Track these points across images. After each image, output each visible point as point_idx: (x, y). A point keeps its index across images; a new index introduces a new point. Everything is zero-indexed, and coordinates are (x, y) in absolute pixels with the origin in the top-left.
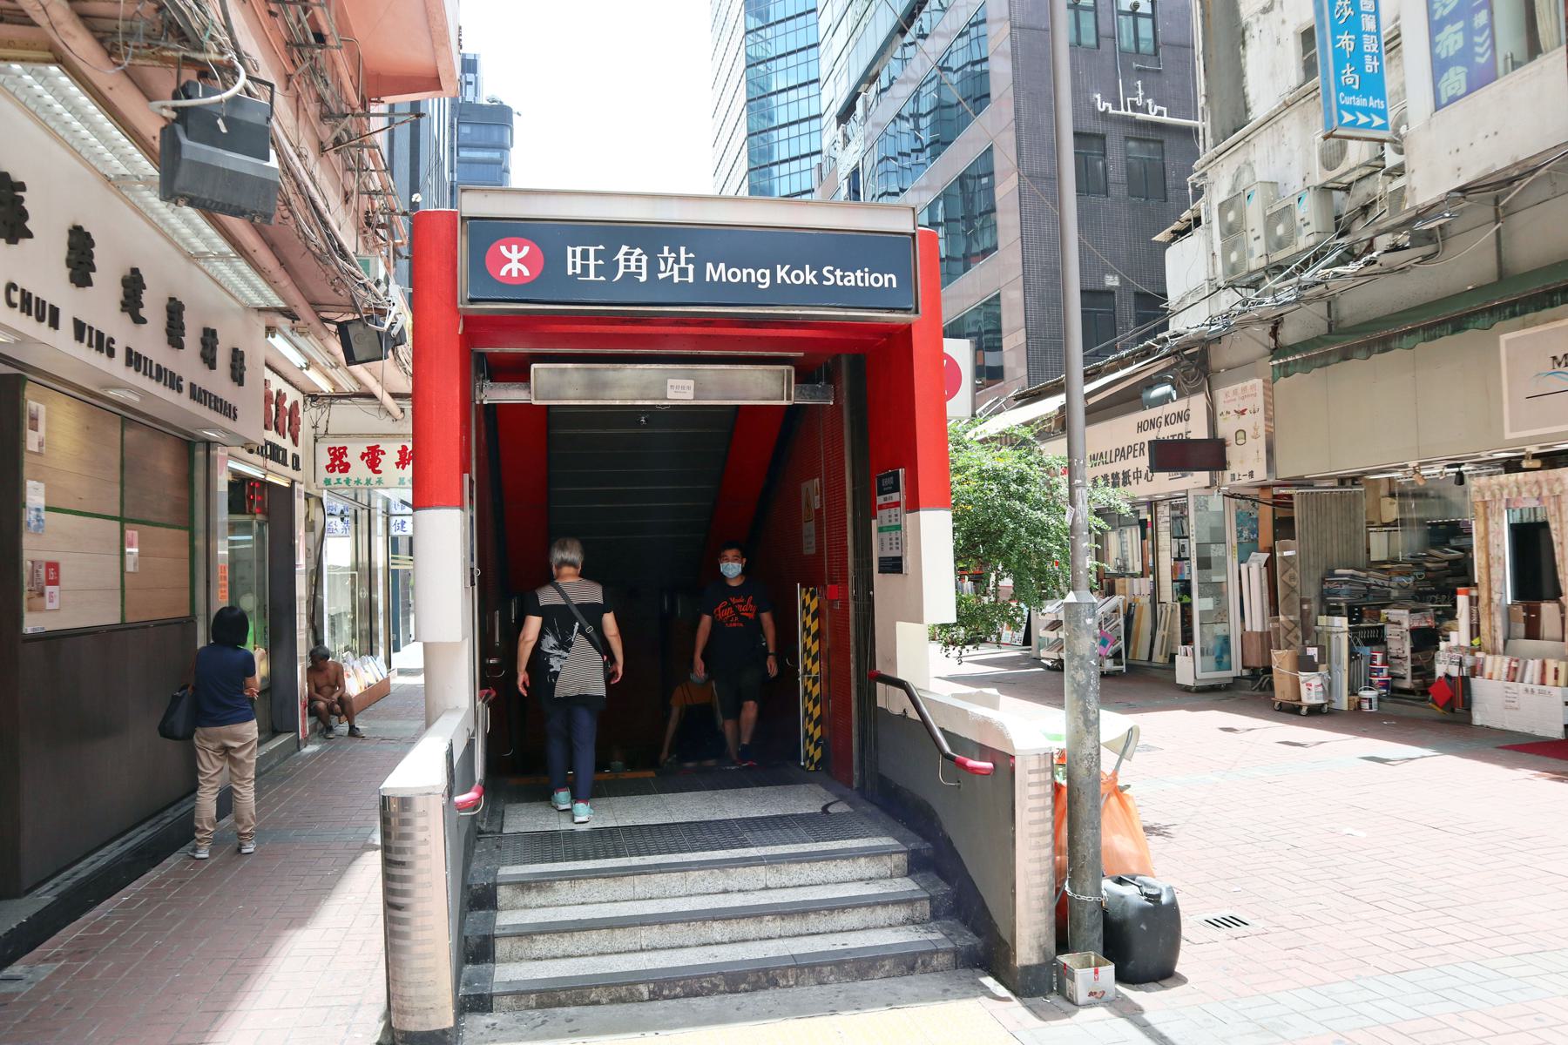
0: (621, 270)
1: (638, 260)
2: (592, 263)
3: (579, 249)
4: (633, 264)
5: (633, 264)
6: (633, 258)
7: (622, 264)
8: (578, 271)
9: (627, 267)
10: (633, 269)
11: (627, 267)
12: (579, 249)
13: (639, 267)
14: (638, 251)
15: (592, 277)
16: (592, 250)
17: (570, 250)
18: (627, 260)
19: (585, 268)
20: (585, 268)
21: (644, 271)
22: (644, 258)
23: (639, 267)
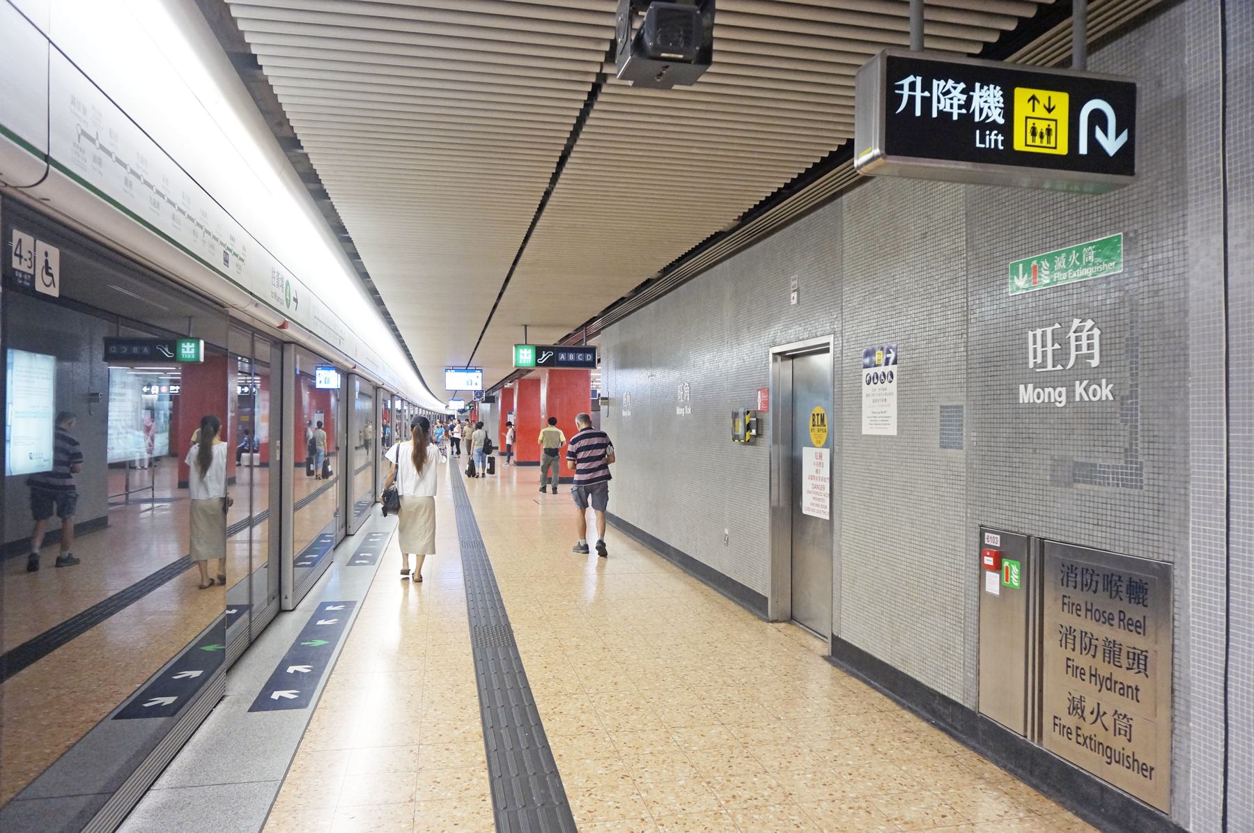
0: (1073, 354)
1: (1090, 337)
2: (1049, 349)
3: (1039, 332)
4: (1084, 342)
5: (1084, 342)
6: (1084, 335)
7: (1073, 344)
8: (1039, 360)
9: (1078, 348)
10: (1084, 350)
11: (1078, 348)
12: (1039, 332)
13: (1090, 346)
14: (1089, 323)
15: (1050, 368)
16: (1049, 330)
17: (1031, 334)
18: (1078, 339)
19: (1044, 354)
20: (1044, 354)
21: (1096, 351)
22: (1096, 332)
23: (1090, 346)
